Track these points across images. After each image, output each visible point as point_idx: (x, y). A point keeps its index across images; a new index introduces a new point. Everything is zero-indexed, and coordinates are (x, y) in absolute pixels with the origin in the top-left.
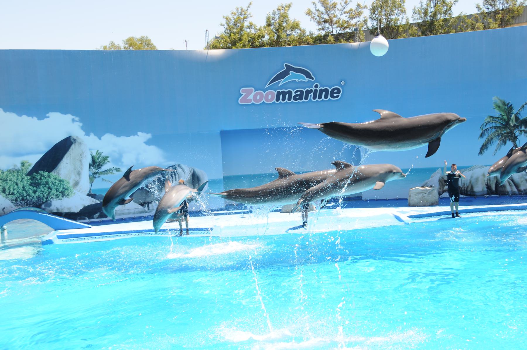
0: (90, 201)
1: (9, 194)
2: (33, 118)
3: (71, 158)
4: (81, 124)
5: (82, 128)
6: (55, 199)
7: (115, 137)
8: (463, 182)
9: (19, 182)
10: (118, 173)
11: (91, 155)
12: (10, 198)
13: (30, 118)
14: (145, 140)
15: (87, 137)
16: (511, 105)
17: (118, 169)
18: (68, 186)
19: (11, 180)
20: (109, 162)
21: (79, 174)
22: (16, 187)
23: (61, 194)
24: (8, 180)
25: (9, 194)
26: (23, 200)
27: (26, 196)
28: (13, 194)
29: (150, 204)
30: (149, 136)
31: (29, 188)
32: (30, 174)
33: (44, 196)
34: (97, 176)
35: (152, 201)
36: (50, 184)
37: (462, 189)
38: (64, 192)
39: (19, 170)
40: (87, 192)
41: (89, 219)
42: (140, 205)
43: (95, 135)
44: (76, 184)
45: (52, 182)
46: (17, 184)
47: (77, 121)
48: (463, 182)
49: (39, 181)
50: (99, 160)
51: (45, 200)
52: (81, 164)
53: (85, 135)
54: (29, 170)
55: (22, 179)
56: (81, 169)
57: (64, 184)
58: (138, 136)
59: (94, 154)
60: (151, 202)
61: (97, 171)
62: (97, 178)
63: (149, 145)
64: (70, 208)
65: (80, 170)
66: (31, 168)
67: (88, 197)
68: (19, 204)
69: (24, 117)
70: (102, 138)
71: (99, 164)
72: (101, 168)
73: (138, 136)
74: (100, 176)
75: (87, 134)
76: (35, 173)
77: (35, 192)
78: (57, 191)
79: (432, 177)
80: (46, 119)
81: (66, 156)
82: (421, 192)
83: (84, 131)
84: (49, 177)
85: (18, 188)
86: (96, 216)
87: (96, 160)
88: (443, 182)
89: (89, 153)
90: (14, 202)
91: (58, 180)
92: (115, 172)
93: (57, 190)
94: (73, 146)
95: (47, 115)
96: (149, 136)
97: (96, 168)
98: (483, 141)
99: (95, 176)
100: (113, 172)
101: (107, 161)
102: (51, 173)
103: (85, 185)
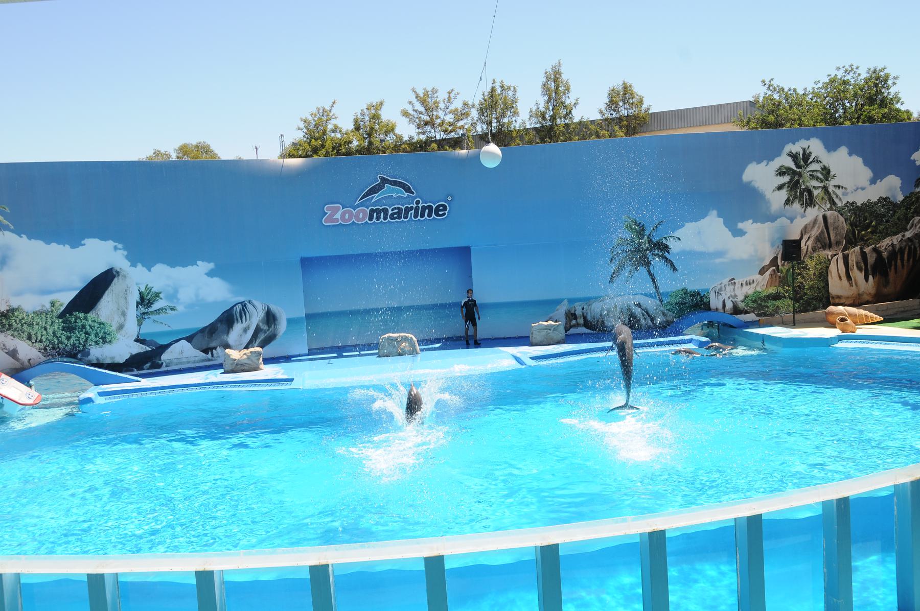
0: (138, 348)
1: (36, 341)
2: (64, 246)
3: (114, 295)
4: (125, 253)
5: (127, 257)
6: (94, 347)
8: (592, 316)
9: (48, 327)
10: (173, 312)
11: (139, 291)
12: (38, 347)
13: (62, 246)
14: (207, 271)
15: (133, 268)
16: (643, 225)
18: (111, 330)
19: (38, 324)
20: (161, 298)
21: (124, 314)
22: (44, 332)
23: (101, 340)
24: (35, 324)
25: (36, 341)
26: (53, 348)
27: (58, 344)
28: (41, 341)
30: (211, 266)
31: (62, 334)
32: (61, 316)
33: (80, 343)
34: (146, 317)
35: (217, 347)
36: (88, 328)
37: (591, 323)
38: (105, 337)
39: (48, 312)
40: (135, 337)
41: (137, 371)
43: (143, 266)
44: (121, 327)
45: (90, 325)
46: (46, 329)
47: (120, 249)
48: (592, 316)
49: (74, 325)
50: (149, 297)
51: (81, 348)
52: (127, 302)
53: (130, 266)
54: (61, 311)
55: (52, 322)
56: (126, 308)
57: (105, 329)
58: (198, 266)
59: (143, 289)
60: (215, 348)
61: (147, 310)
63: (212, 277)
64: (113, 358)
65: (125, 310)
66: (62, 309)
67: (136, 342)
68: (48, 354)
69: (54, 245)
70: (152, 269)
72: (151, 306)
73: (198, 266)
75: (134, 265)
76: (68, 315)
77: (68, 338)
78: (96, 337)
79: (557, 310)
80: (80, 247)
81: (107, 292)
82: (545, 328)
83: (129, 261)
84: (86, 319)
85: (47, 333)
88: (571, 317)
89: (137, 288)
90: (43, 351)
91: (97, 323)
92: (169, 311)
93: (96, 335)
94: (116, 280)
95: (83, 242)
96: (211, 266)
98: (613, 267)
102: (89, 315)
103: (132, 327)
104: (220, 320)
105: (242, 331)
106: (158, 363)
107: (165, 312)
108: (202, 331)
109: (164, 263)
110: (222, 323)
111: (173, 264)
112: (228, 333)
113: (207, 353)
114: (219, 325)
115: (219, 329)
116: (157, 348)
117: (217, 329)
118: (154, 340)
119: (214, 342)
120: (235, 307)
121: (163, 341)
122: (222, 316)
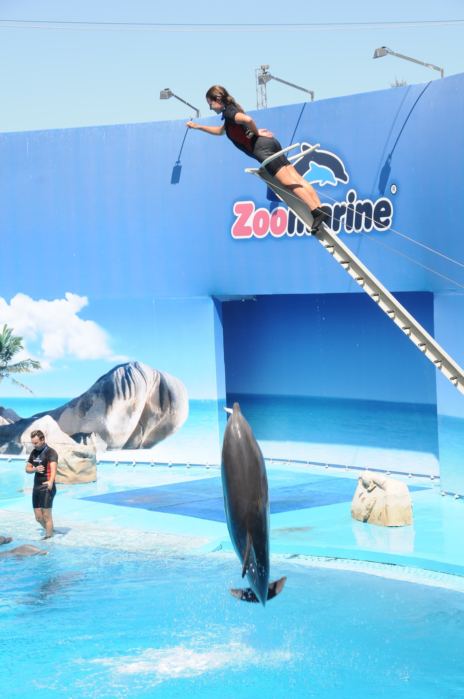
7: (31, 300)
10: (36, 369)
14: (78, 310)
17: (36, 363)
20: (22, 347)
29: (87, 438)
30: (84, 301)
35: (91, 433)
42: (71, 438)
50: (7, 344)
58: (67, 300)
60: (89, 435)
61: (5, 363)
62: (5, 377)
63: (85, 320)
70: (12, 301)
71: (8, 350)
72: (10, 358)
73: (67, 300)
74: (10, 373)
86: (3, 449)
87: (3, 343)
92: (31, 368)
96: (84, 301)
97: (4, 359)
99: (2, 374)
100: (29, 368)
101: (20, 347)
104: (95, 390)
105: (125, 412)
106: (17, 445)
107: (27, 370)
108: (72, 404)
109: (25, 293)
110: (98, 396)
111: (36, 298)
112: (106, 413)
113: (78, 441)
114: (94, 398)
115: (94, 405)
116: (16, 423)
117: (92, 405)
118: (12, 409)
119: (87, 425)
120: (115, 372)
121: (24, 414)
122: (98, 384)
